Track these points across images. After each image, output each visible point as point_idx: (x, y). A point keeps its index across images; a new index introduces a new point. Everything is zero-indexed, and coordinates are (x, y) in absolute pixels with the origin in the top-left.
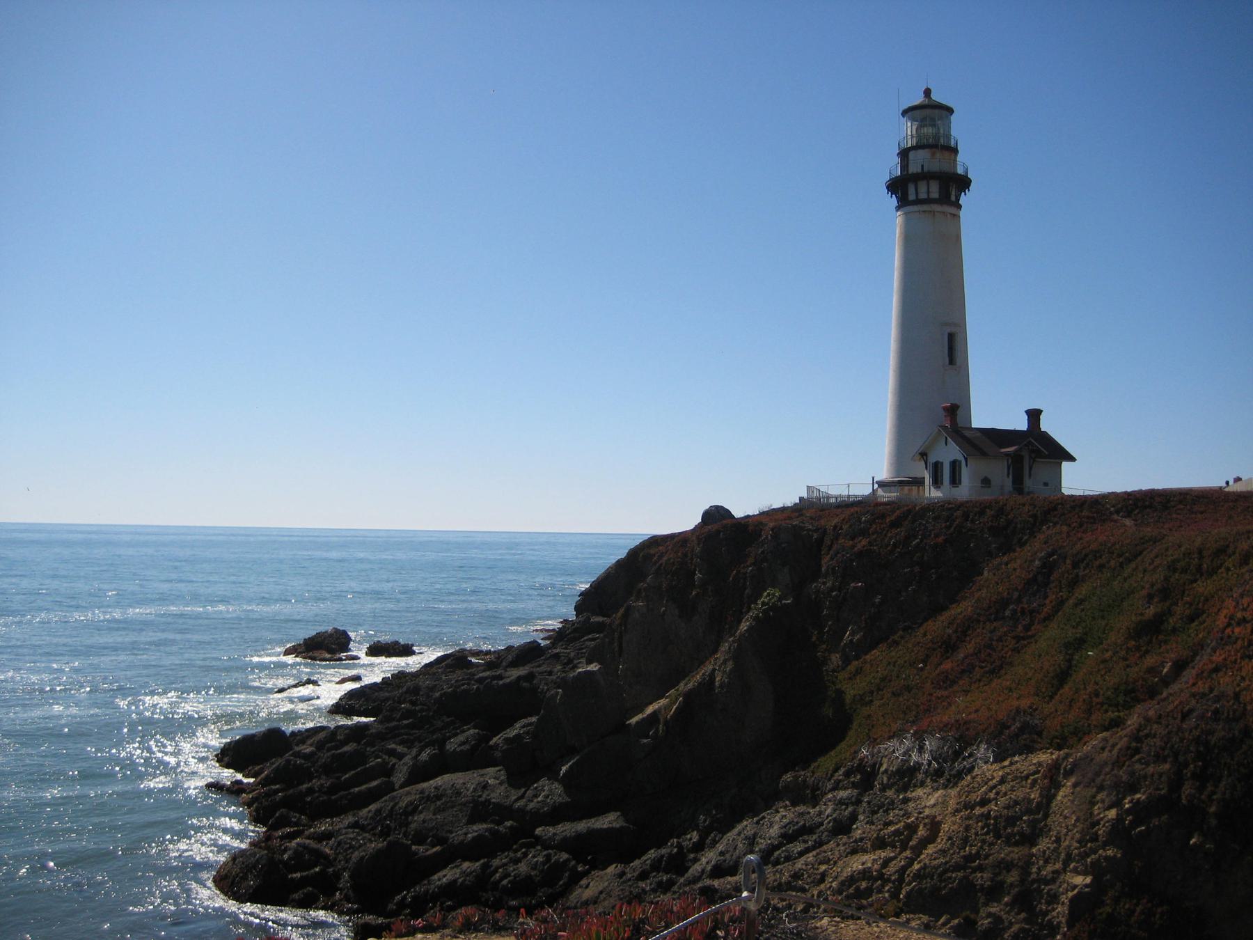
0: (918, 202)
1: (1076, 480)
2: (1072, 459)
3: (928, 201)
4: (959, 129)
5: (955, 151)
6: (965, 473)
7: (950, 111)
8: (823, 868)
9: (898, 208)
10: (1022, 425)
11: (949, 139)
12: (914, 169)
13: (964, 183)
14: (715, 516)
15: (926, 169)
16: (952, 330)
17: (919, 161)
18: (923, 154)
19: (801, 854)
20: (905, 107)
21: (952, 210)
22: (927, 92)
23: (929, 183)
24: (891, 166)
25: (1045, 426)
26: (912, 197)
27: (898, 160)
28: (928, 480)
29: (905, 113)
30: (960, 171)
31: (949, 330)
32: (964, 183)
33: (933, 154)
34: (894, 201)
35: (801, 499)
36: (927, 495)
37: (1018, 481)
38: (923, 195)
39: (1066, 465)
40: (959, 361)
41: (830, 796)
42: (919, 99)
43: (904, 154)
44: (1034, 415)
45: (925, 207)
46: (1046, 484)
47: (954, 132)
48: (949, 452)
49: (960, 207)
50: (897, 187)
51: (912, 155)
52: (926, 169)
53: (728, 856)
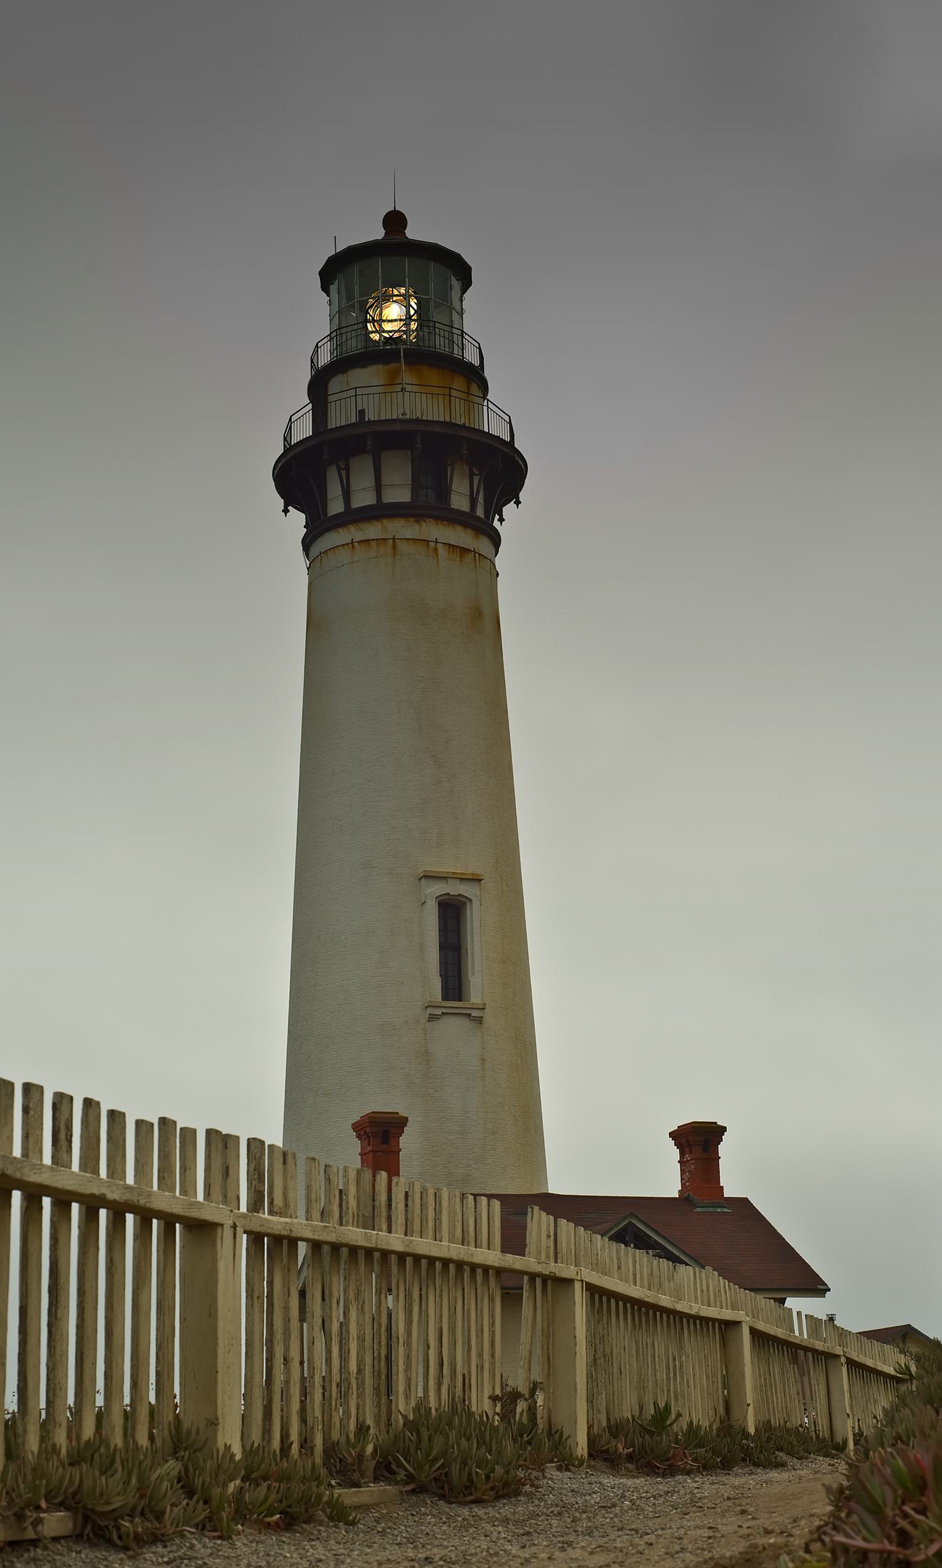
3: (380, 512)
10: (663, 1178)
18: (368, 377)
23: (401, 465)
25: (733, 1183)
26: (336, 507)
31: (438, 889)
38: (363, 498)
44: (699, 1143)
45: (373, 530)
50: (300, 477)
51: (335, 385)
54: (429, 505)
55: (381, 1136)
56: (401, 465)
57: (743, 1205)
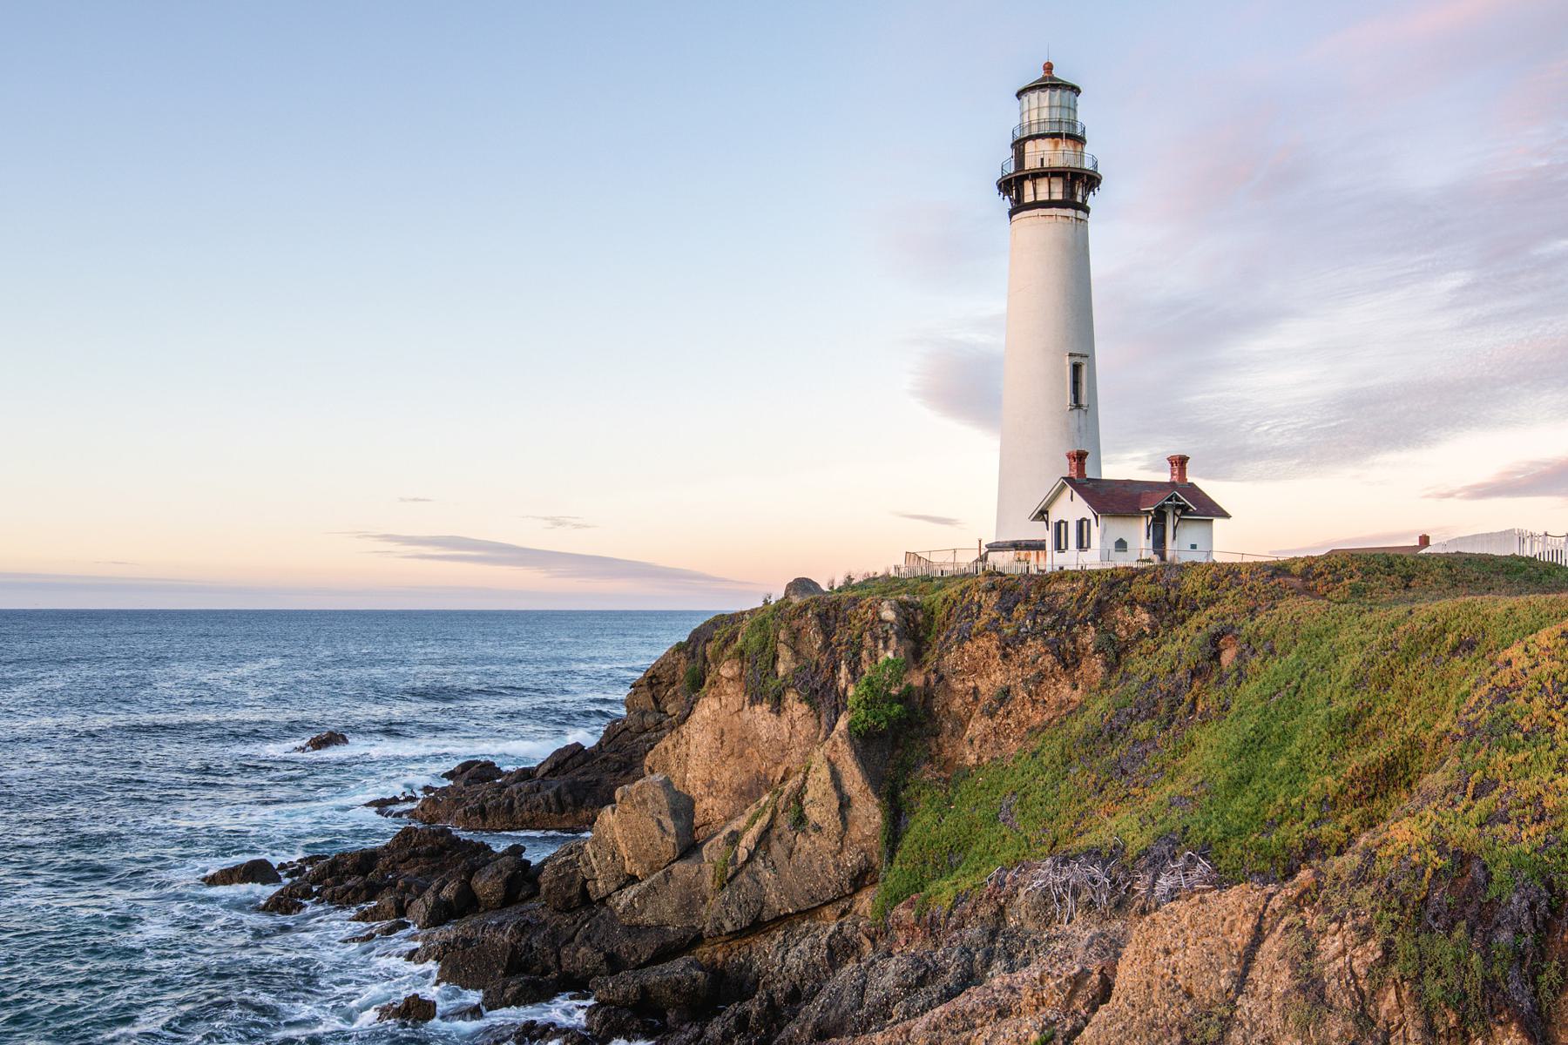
0: (1036, 205)
1: (1228, 543)
2: (1224, 515)
4: (1087, 115)
5: (1079, 140)
6: (1095, 532)
7: (1075, 90)
8: (967, 1034)
9: (1012, 213)
11: (1075, 127)
12: (1031, 163)
13: (1091, 181)
14: (802, 585)
15: (1046, 165)
16: (1077, 360)
17: (1039, 154)
18: (1045, 145)
19: (923, 1010)
20: (1021, 87)
21: (1081, 214)
22: (1049, 67)
23: (1052, 181)
24: (1001, 161)
26: (1029, 198)
27: (1010, 153)
28: (1049, 545)
29: (1020, 94)
30: (1088, 165)
32: (1091, 181)
33: (1056, 144)
34: (1007, 204)
35: (897, 568)
36: (1049, 561)
37: (1159, 544)
38: (1043, 196)
39: (1217, 522)
40: (1084, 402)
41: (956, 934)
42: (1041, 74)
43: (1019, 146)
44: (1180, 462)
45: (1047, 211)
46: (1193, 547)
47: (1081, 117)
48: (1072, 508)
49: (1087, 210)
50: (1011, 185)
51: (1029, 147)
52: (1046, 165)
53: (832, 1012)
54: (1068, 203)
55: (1080, 457)
56: (1052, 181)
57: (1192, 484)
